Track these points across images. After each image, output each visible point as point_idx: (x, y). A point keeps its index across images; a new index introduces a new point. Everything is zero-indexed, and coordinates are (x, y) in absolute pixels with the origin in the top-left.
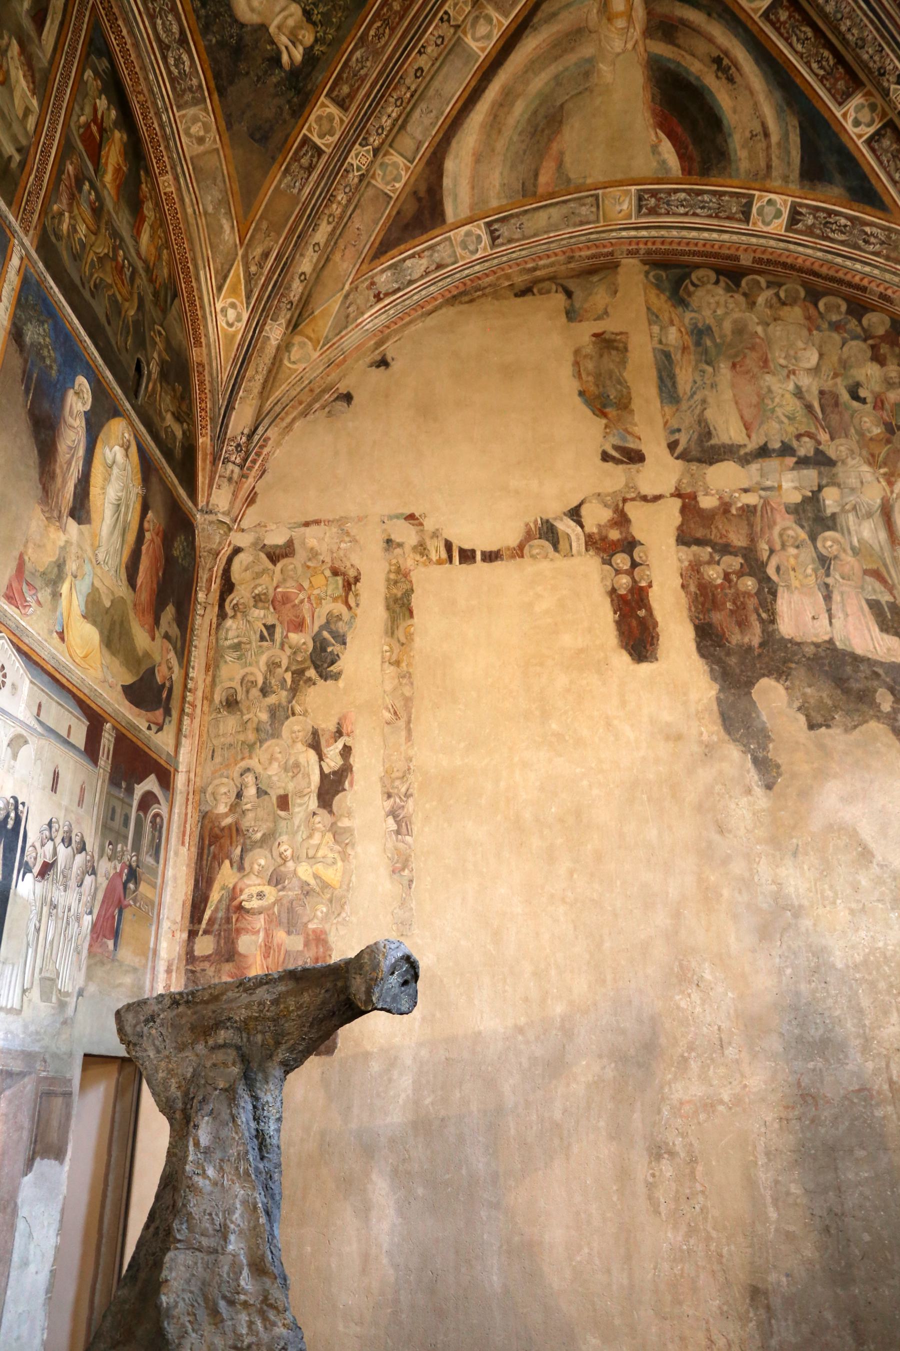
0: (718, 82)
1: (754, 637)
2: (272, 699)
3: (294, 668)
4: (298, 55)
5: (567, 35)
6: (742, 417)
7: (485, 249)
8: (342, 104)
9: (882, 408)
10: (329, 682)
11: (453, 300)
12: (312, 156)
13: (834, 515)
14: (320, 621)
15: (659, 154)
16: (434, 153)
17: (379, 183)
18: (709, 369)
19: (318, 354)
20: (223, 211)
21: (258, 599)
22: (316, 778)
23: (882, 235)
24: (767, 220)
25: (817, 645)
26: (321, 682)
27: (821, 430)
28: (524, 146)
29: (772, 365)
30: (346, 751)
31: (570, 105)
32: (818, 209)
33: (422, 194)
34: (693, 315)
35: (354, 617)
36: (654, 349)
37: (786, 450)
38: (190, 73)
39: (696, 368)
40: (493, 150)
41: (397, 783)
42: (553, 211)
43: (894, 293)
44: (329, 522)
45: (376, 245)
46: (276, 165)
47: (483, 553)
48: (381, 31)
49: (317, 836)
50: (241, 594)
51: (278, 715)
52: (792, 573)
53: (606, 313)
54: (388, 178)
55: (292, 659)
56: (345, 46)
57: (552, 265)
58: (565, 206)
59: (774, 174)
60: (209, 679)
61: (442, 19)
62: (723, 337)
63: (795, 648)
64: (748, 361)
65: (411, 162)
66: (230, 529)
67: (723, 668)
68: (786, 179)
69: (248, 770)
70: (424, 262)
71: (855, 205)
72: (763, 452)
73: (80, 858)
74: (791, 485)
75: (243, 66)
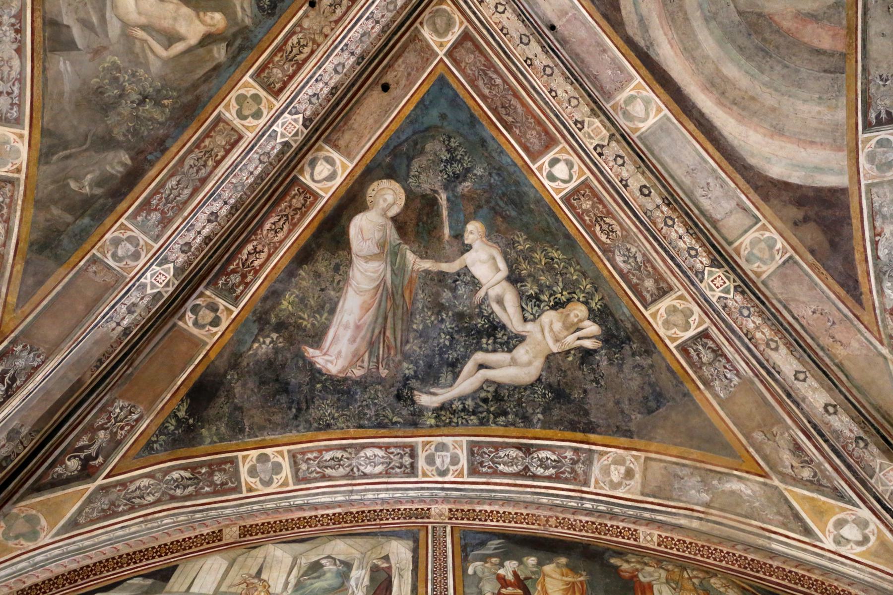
4: (592, 328)
8: (663, 291)
12: (704, 346)
16: (756, 189)
17: (768, 269)
20: (715, 482)
28: (778, 68)
38: (559, 455)
40: (774, 110)
42: (872, 31)
45: (843, 293)
46: (696, 395)
48: (605, 227)
54: (766, 256)
56: (605, 273)
58: (871, 12)
61: (600, 155)
65: (758, 220)
75: (576, 394)
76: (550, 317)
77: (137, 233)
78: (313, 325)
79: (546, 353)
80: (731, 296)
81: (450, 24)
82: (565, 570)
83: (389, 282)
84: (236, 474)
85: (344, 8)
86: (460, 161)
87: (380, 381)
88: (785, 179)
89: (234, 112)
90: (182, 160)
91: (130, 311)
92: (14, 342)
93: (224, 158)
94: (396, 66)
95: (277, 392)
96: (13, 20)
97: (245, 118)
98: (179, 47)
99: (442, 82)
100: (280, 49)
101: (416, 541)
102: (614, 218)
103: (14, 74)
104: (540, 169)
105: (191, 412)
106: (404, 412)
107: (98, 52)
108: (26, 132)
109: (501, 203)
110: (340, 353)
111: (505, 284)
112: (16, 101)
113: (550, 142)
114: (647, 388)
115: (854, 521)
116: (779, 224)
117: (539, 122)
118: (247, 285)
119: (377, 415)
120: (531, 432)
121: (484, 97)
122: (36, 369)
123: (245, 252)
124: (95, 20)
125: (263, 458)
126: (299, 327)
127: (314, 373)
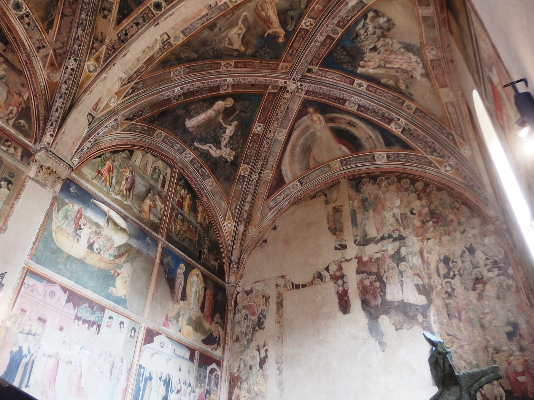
1: (379, 302)
2: (247, 337)
3: (253, 327)
4: (232, 158)
6: (376, 228)
7: (299, 187)
8: (248, 164)
9: (421, 216)
10: (262, 330)
11: (293, 204)
13: (404, 256)
14: (259, 312)
16: (278, 167)
17: (264, 179)
18: (366, 213)
21: (244, 307)
22: (258, 360)
23: (415, 157)
24: (381, 159)
25: (398, 302)
26: (260, 330)
27: (401, 228)
29: (386, 208)
30: (266, 350)
31: (312, 144)
33: (277, 178)
34: (362, 195)
35: (268, 310)
36: (350, 209)
37: (390, 236)
39: (363, 213)
41: (279, 359)
42: (316, 171)
44: (261, 281)
47: (302, 285)
49: (259, 377)
50: (240, 306)
51: (249, 341)
52: (391, 278)
53: (337, 200)
55: (252, 325)
60: (232, 333)
62: (371, 201)
63: (392, 304)
64: (378, 208)
66: (236, 287)
67: (370, 313)
68: (382, 147)
69: (242, 359)
70: (282, 196)
72: (383, 238)
73: (189, 388)
74: (391, 248)
77: (182, 71)
86: (247, 110)
87: (192, 134)
91: (167, 96)
92: (141, 81)
98: (230, 47)
99: (262, 95)
100: (246, 62)
103: (196, 27)
106: (190, 143)
107: (215, 35)
108: (185, 39)
113: (263, 123)
116: (273, 175)
118: (190, 97)
122: (140, 89)
125: (161, 133)
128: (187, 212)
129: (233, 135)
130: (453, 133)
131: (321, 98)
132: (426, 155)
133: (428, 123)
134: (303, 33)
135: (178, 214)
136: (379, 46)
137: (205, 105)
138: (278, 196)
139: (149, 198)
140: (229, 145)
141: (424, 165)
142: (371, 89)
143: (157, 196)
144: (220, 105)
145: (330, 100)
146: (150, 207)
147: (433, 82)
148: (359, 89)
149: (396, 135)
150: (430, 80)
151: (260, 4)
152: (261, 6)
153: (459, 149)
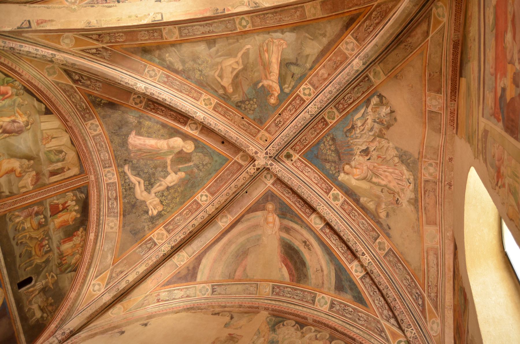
0: (305, 249)
4: (155, 212)
5: (253, 226)
8: (168, 231)
12: (152, 245)
15: (282, 272)
16: (199, 256)
19: (123, 314)
20: (110, 252)
24: (322, 305)
32: (341, 303)
33: (190, 268)
34: (275, 335)
38: (115, 208)
40: (221, 260)
42: (239, 286)
43: (365, 343)
45: (166, 282)
46: (137, 243)
53: (241, 328)
54: (179, 260)
57: (232, 307)
59: (325, 286)
65: (190, 257)
68: (329, 289)
70: (182, 293)
71: (356, 303)
75: (134, 211)
76: (157, 200)
77: (159, 75)
78: (143, 132)
79: (146, 200)
80: (162, 253)
81: (244, 161)
82: (74, 218)
83: (161, 152)
84: (90, 120)
85: (243, 128)
87: (129, 154)
88: (201, 264)
89: (205, 98)
90: (185, 85)
92: (111, 50)
93: (190, 96)
94: (230, 145)
95: (118, 126)
96: (211, 30)
97: (204, 101)
98: (219, 80)
100: (227, 109)
101: (79, 174)
102: (191, 215)
103: (196, 33)
104: (204, 192)
105: (104, 104)
106: (121, 163)
108: (179, 39)
109: (192, 182)
110: (135, 141)
111: (166, 186)
112: (187, 35)
113: (212, 194)
114: (138, 230)
115: (100, 288)
116: (188, 263)
117: (218, 190)
119: (118, 155)
120: (121, 199)
121: (224, 173)
122: (104, 58)
123: (162, 108)
124: (219, 54)
126: (141, 128)
127: (127, 135)
128: (57, 225)
129: (172, 186)
130: (425, 295)
131: (287, 197)
132: (380, 318)
133: (397, 274)
134: (298, 102)
135: (42, 213)
136: (373, 149)
137: (162, 131)
138: (177, 289)
139: (21, 163)
140: (161, 195)
141: (373, 331)
142: (346, 207)
143: (34, 173)
144: (177, 142)
145: (295, 204)
146: (12, 171)
147: (420, 214)
148: (333, 202)
149: (354, 279)
150: (417, 211)
151: (267, 41)
152: (267, 44)
153: (427, 323)
